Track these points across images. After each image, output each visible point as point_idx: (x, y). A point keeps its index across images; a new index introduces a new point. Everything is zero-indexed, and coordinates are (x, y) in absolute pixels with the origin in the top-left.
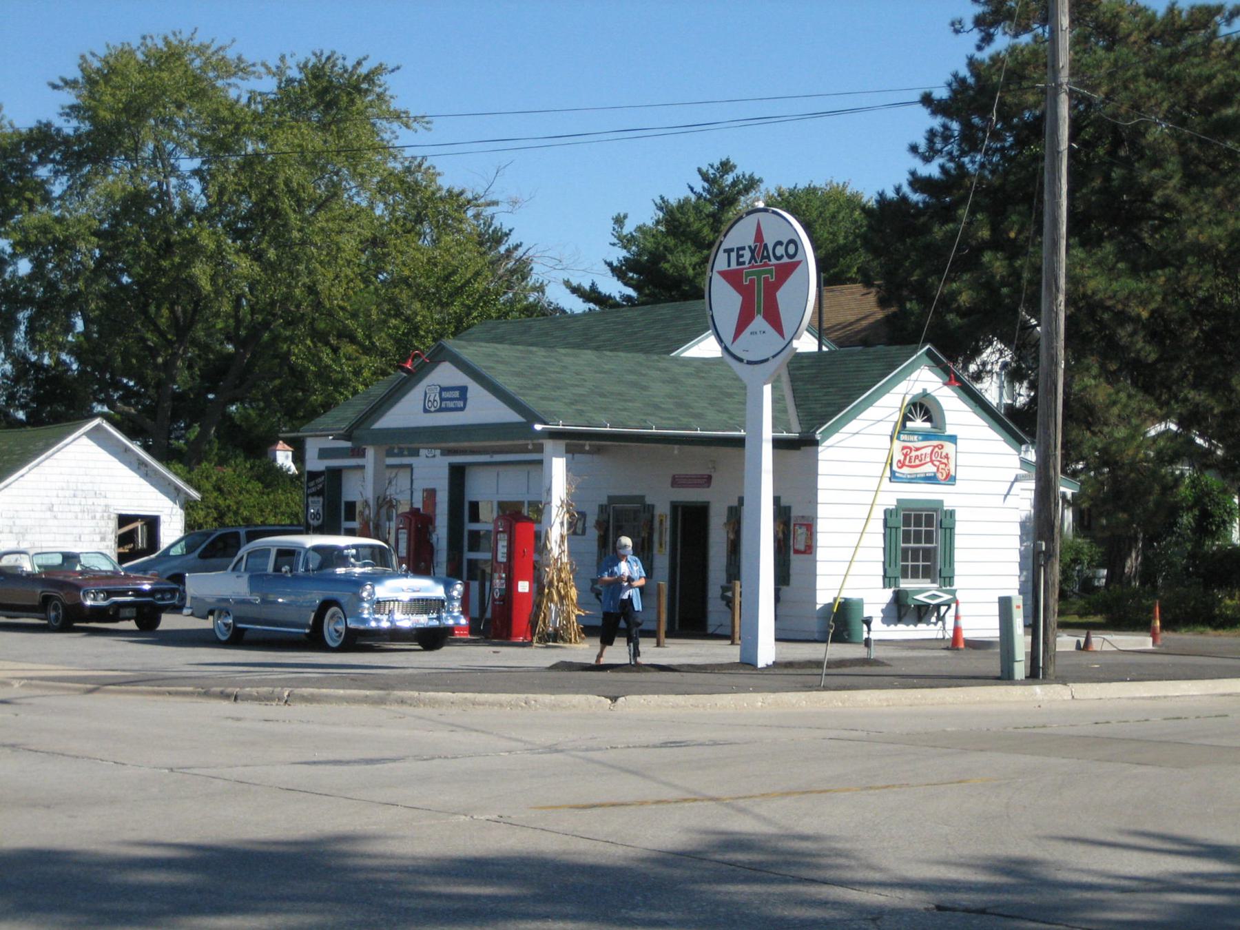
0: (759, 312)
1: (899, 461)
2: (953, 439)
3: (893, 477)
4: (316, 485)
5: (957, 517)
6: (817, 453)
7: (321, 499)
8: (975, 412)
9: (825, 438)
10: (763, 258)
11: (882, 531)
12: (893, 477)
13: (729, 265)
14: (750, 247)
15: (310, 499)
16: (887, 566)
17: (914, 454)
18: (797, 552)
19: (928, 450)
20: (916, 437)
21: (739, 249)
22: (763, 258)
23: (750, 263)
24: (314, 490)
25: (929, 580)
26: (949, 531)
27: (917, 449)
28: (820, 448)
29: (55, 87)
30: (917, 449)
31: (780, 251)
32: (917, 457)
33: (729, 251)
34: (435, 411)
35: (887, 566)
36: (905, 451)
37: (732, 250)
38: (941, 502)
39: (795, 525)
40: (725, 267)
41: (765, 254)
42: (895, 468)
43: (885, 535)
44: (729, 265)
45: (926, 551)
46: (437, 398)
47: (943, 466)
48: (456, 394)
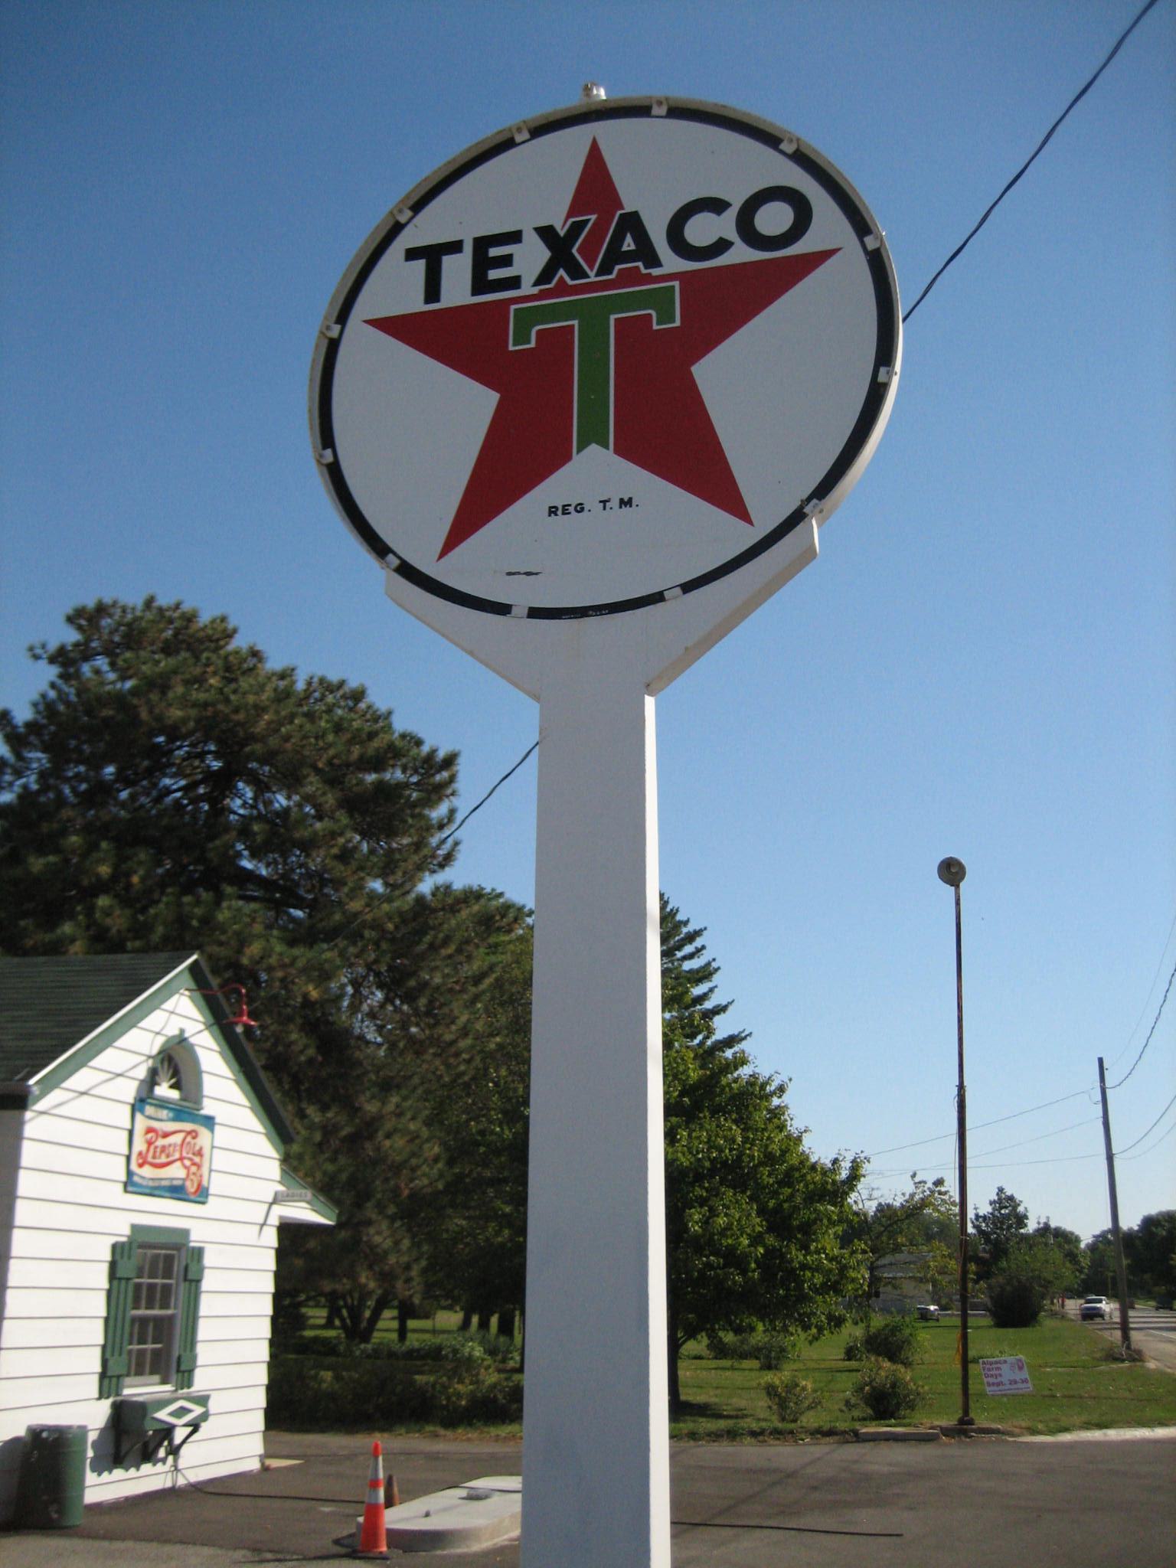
0: (593, 435)
1: (140, 1154)
2: (209, 1122)
3: (130, 1185)
5: (208, 1260)
6: (20, 1124)
8: (237, 1082)
9: (44, 1094)
10: (615, 255)
11: (106, 1286)
12: (130, 1185)
13: (432, 291)
14: (546, 233)
16: (108, 1355)
17: (161, 1142)
19: (177, 1139)
20: (165, 1112)
21: (482, 244)
22: (615, 255)
23: (545, 277)
25: (156, 1378)
26: (193, 1283)
27: (166, 1135)
28: (28, 1115)
30: (166, 1135)
31: (701, 230)
32: (163, 1149)
33: (432, 256)
35: (108, 1355)
36: (149, 1135)
37: (455, 247)
38: (185, 1233)
40: (414, 302)
41: (629, 244)
42: (134, 1167)
43: (109, 1293)
44: (432, 291)
45: (158, 1321)
47: (194, 1169)
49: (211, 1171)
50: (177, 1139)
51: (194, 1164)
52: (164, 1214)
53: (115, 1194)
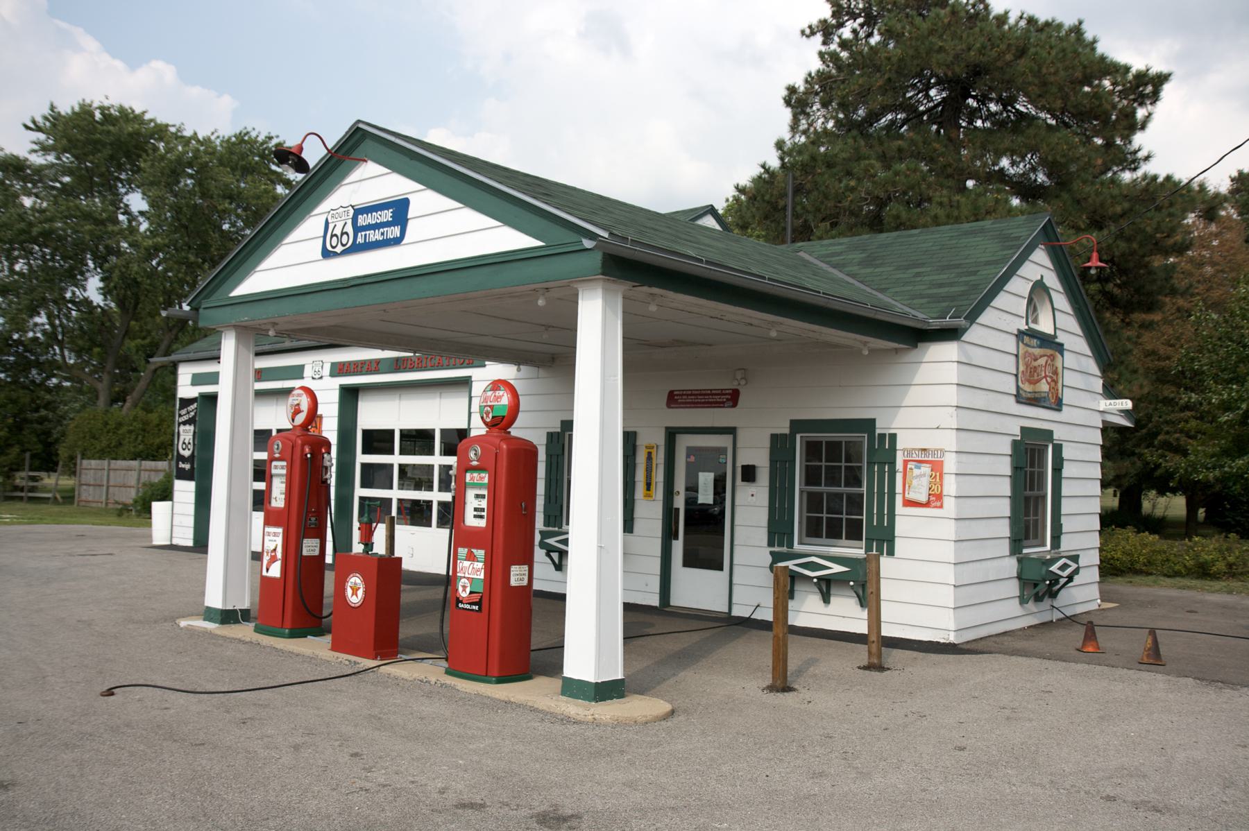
1: (1023, 372)
4: (188, 413)
7: (192, 428)
15: (182, 428)
18: (909, 503)
24: (186, 418)
29: (27, 127)
34: (344, 253)
38: (1050, 433)
39: (906, 462)
42: (1020, 384)
46: (349, 229)
48: (387, 215)
49: (1063, 386)
50: (1042, 361)
51: (1053, 380)
52: (1039, 418)
53: (1011, 405)
